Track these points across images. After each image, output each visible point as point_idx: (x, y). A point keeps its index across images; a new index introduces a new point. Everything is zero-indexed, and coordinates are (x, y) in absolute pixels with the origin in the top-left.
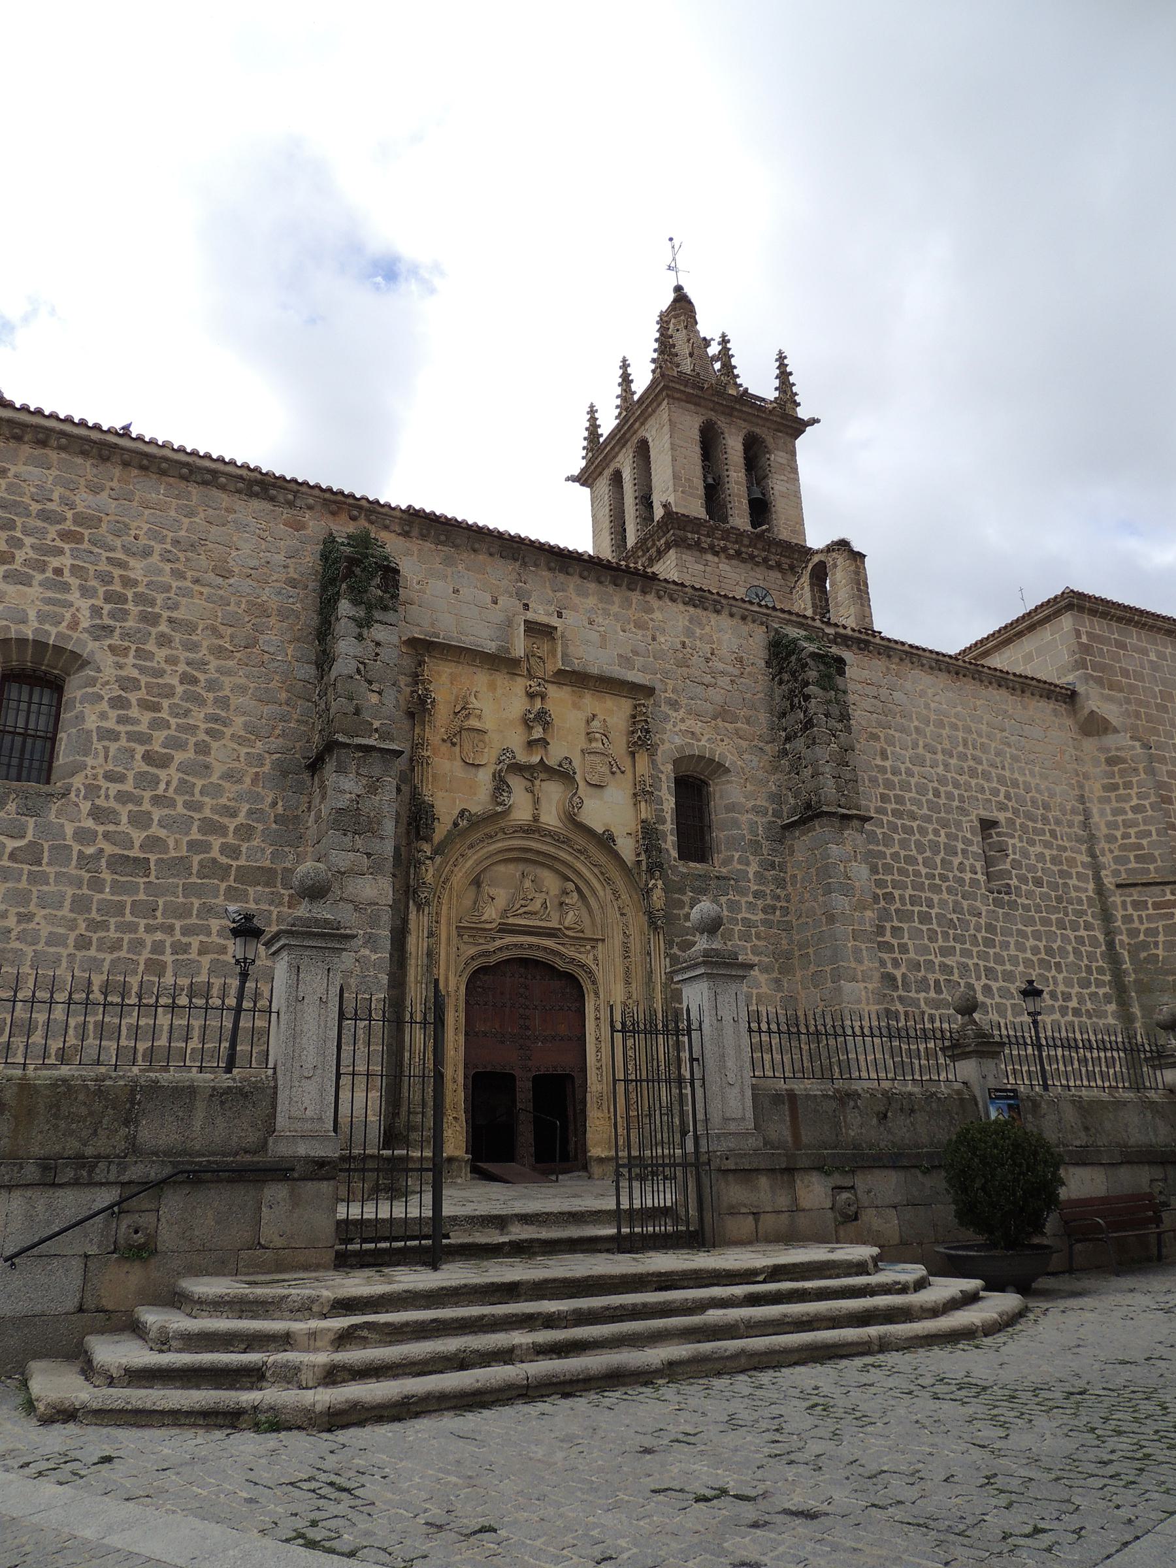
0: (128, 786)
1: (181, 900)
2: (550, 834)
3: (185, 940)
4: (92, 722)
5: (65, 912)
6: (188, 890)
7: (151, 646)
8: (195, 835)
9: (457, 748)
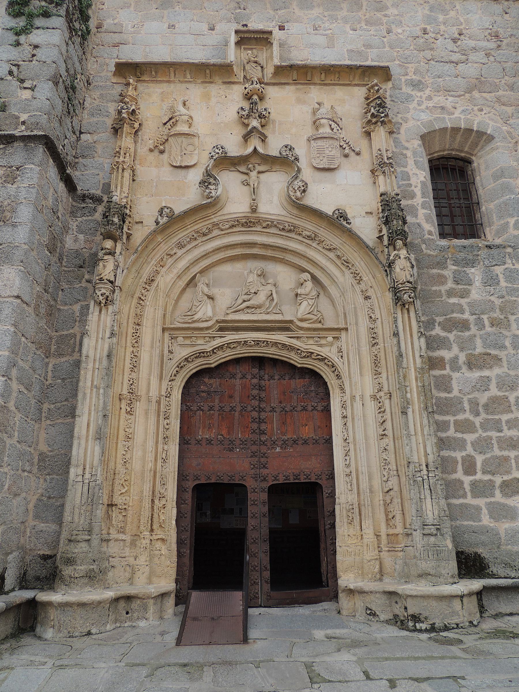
2: (271, 224)
9: (165, 156)
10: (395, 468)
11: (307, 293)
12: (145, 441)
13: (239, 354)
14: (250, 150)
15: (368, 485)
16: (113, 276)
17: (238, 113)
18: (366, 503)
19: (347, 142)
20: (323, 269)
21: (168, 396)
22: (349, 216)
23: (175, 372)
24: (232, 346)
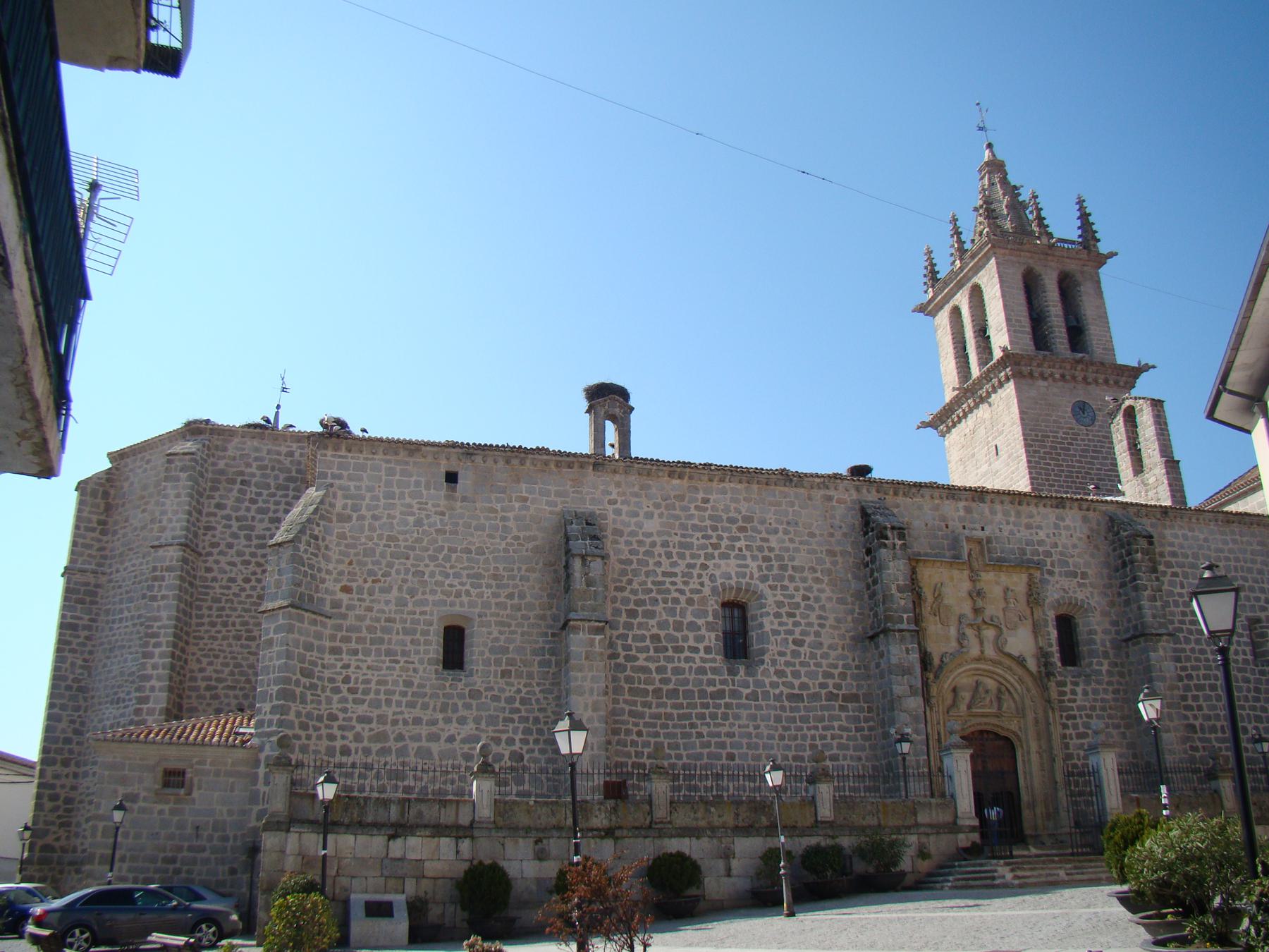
0: (788, 658)
1: (820, 713)
3: (824, 733)
4: (767, 627)
5: (772, 723)
6: (823, 708)
7: (786, 583)
8: (821, 680)
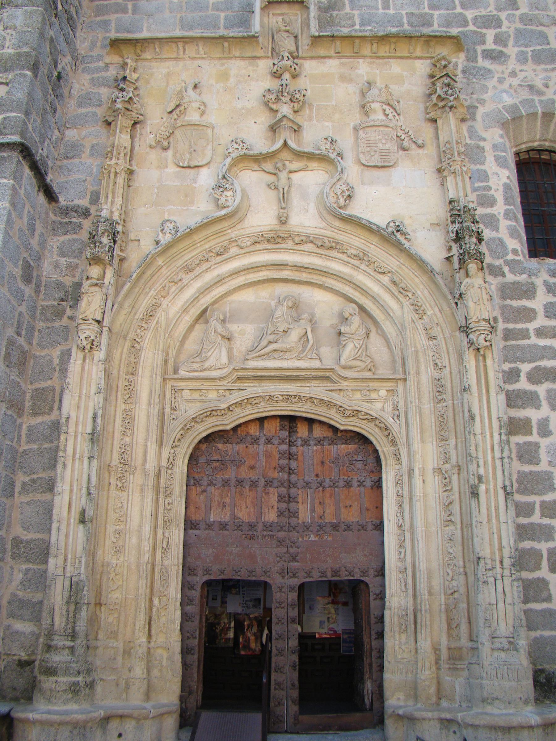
9: (170, 153)
10: (461, 563)
11: (353, 332)
12: (140, 526)
13: (262, 412)
14: (279, 144)
15: (426, 584)
16: (100, 314)
17: (264, 96)
18: (423, 609)
19: (407, 131)
20: (375, 299)
21: (171, 465)
22: (409, 230)
23: (179, 436)
24: (254, 402)
